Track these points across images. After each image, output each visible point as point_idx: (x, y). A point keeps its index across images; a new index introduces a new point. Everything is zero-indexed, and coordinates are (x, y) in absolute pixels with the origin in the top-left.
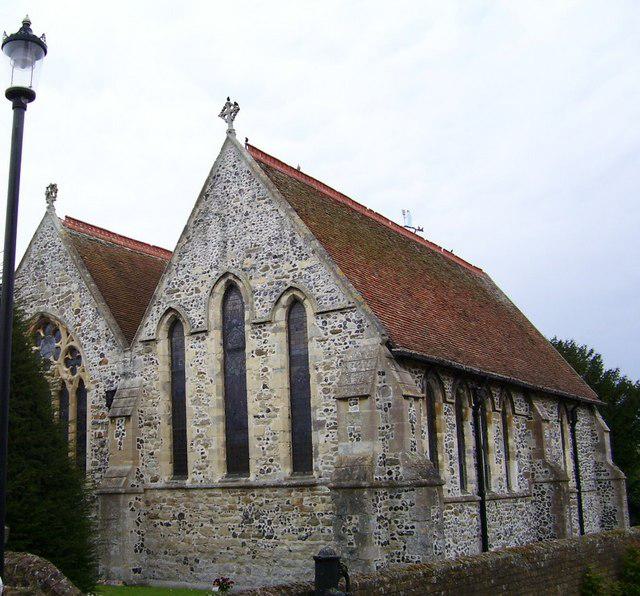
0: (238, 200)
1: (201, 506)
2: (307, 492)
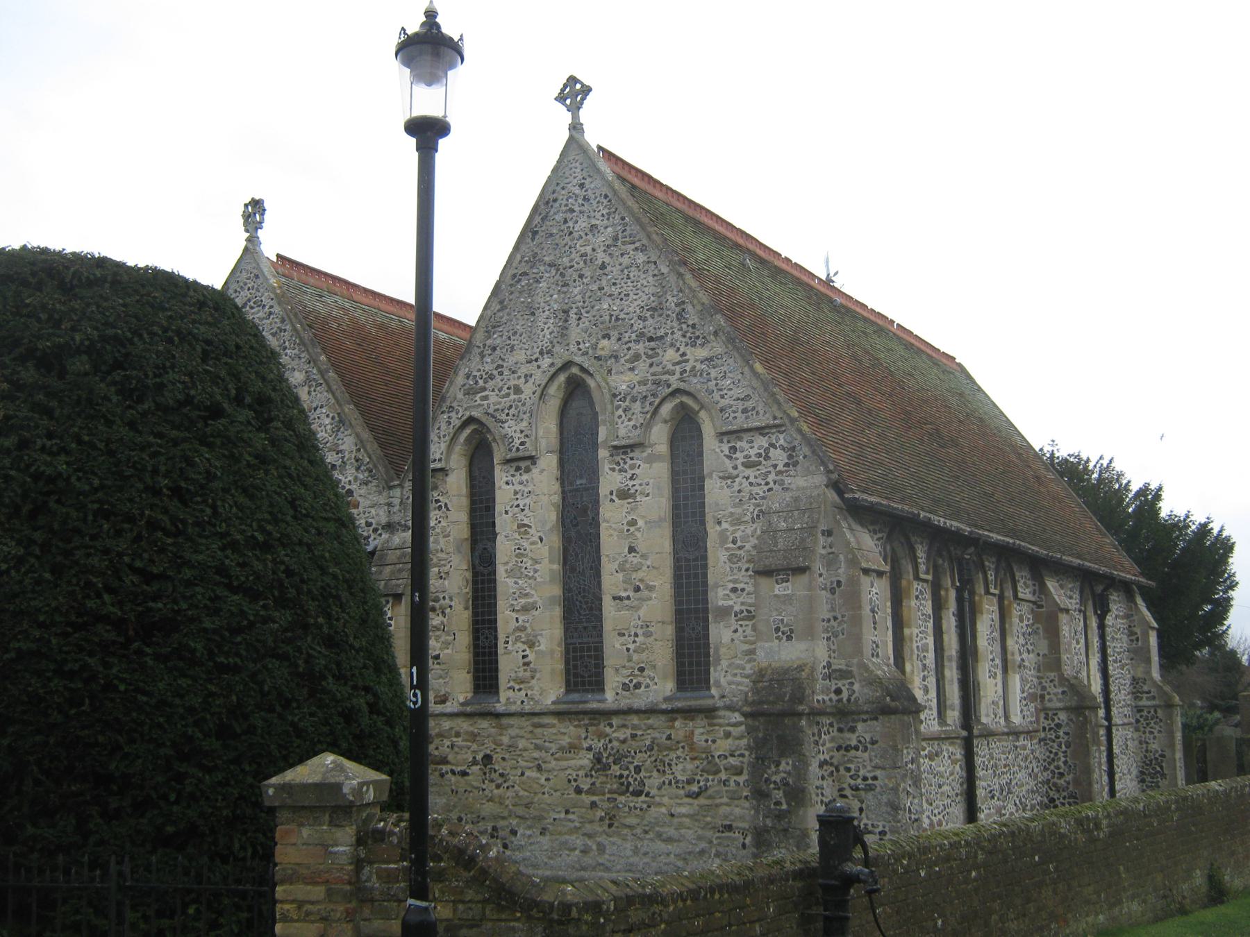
0: (587, 243)
1: (522, 744)
2: (701, 721)
